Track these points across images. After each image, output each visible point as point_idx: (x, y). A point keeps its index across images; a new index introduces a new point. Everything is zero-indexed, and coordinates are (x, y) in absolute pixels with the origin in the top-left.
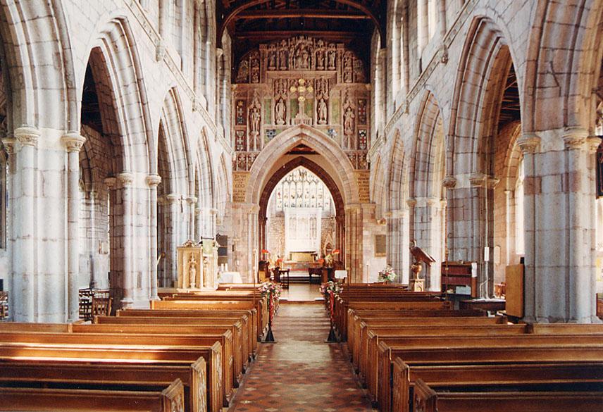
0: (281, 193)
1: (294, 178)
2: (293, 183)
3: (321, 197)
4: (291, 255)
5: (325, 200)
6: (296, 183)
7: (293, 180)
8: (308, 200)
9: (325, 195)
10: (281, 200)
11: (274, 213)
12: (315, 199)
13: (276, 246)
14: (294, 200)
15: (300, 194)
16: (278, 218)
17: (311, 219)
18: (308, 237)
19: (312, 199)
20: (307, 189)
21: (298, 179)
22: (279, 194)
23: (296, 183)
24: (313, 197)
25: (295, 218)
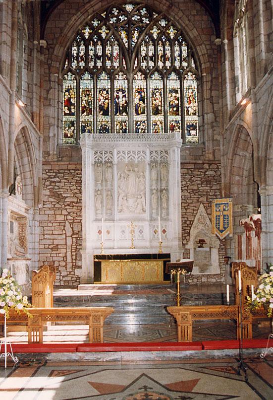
0: (73, 101)
1: (108, 63)
2: (104, 76)
3: (179, 109)
4: (97, 267)
5: (187, 118)
6: (112, 78)
7: (104, 68)
8: (143, 117)
9: (186, 105)
10: (73, 118)
11: (52, 147)
12: (160, 117)
13: (60, 241)
14: (108, 118)
15: (122, 101)
16: (63, 164)
17: (153, 164)
18: (147, 216)
19: (154, 118)
20: (140, 91)
21: (116, 64)
22: (68, 103)
23: (112, 78)
24: (157, 112)
25: (109, 164)
